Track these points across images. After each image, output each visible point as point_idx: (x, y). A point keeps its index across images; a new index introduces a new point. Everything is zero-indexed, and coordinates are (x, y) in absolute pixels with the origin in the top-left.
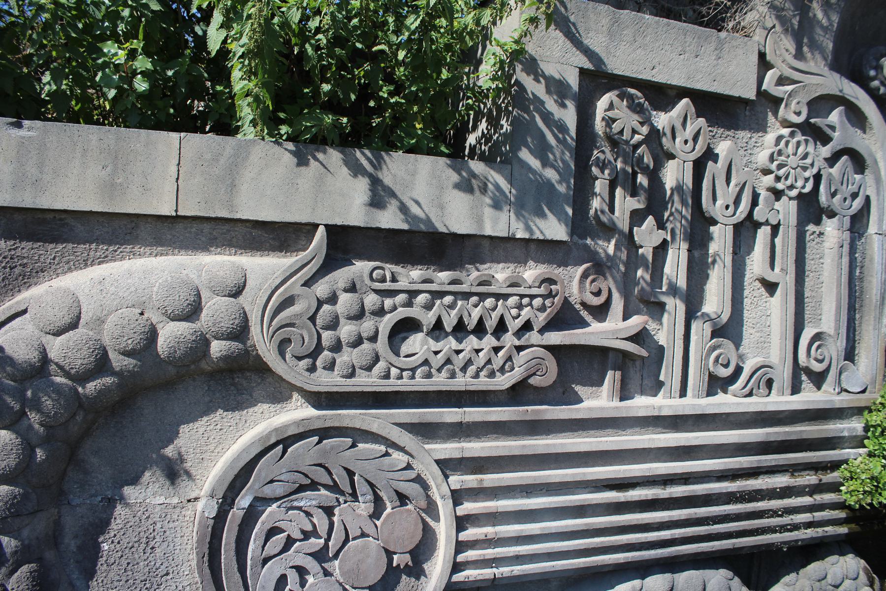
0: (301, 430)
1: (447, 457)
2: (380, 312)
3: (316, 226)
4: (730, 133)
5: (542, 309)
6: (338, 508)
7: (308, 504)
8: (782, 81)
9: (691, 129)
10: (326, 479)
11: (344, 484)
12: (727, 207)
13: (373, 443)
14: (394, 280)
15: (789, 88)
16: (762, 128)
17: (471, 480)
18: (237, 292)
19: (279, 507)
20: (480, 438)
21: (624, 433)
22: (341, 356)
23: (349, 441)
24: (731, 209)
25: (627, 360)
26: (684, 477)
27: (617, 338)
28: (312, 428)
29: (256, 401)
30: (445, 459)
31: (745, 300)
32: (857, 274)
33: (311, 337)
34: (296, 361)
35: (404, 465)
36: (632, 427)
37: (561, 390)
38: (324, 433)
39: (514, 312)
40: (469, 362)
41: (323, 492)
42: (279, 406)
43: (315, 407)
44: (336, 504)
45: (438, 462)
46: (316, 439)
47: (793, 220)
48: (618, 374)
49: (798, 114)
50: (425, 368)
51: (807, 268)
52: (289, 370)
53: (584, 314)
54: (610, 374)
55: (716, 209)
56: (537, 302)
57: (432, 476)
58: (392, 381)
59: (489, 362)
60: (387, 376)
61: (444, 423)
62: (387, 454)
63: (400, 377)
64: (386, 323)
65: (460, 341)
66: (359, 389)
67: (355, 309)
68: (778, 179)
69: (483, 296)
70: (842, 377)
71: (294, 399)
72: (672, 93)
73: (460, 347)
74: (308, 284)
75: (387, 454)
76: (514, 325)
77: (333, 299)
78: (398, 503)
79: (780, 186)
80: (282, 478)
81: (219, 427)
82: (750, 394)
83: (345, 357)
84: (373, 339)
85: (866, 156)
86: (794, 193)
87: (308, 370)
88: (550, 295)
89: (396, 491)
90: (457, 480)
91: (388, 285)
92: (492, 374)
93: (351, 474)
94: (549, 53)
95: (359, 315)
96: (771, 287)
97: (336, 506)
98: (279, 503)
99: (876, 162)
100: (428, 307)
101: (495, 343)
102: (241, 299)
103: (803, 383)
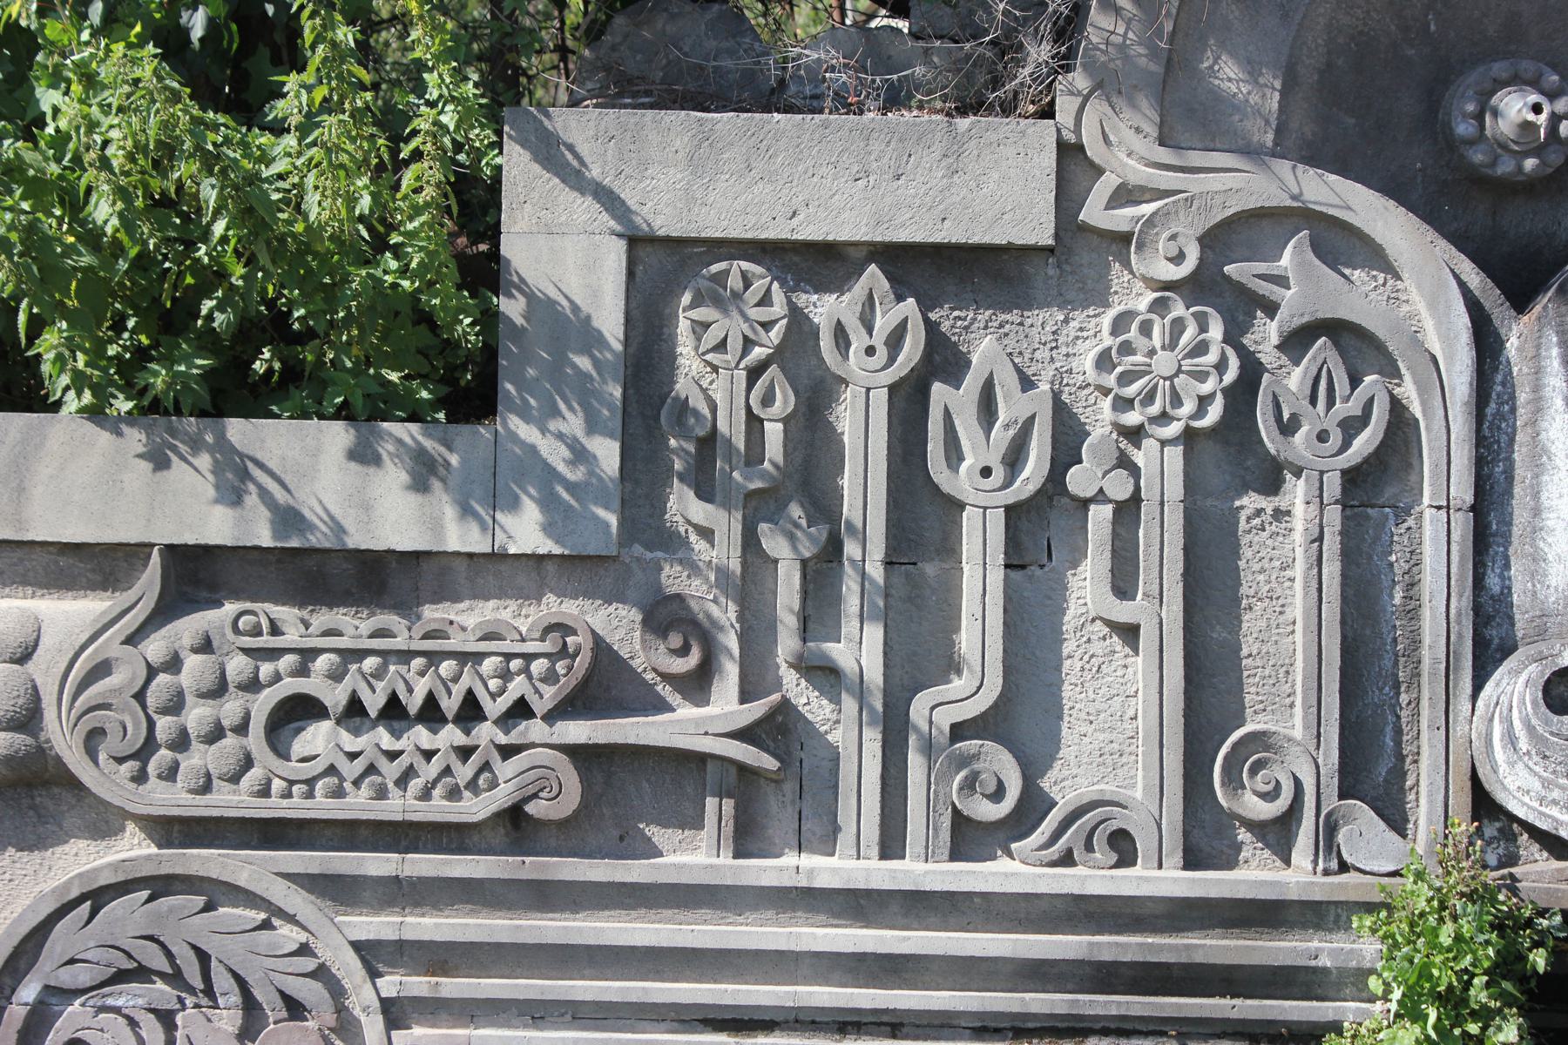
0: (121, 878)
1: (371, 937)
2: (253, 685)
3: (153, 545)
4: (1014, 316)
5: (550, 677)
6: (181, 1014)
7: (131, 1003)
8: (1125, 195)
9: (883, 323)
10: (161, 963)
11: (194, 978)
12: (986, 472)
13: (246, 907)
14: (275, 630)
15: (1147, 209)
16: (1101, 299)
17: (419, 985)
18: (24, 656)
19: (83, 1005)
20: (440, 910)
21: (740, 919)
22: (189, 758)
23: (200, 901)
24: (999, 474)
25: (762, 781)
26: (885, 1019)
27: (706, 733)
28: (138, 875)
29: (67, 834)
30: (368, 941)
31: (1067, 663)
32: (1397, 600)
33: (136, 725)
34: (113, 765)
35: (295, 947)
36: (755, 908)
37: (616, 833)
38: (162, 886)
39: (494, 684)
40: (409, 773)
41: (160, 985)
42: (104, 843)
43: (160, 847)
44: (178, 1006)
45: (357, 946)
46: (145, 894)
47: (1175, 488)
48: (728, 805)
49: (1178, 258)
50: (332, 781)
51: (1244, 590)
52: (102, 779)
53: (665, 690)
54: (711, 803)
55: (961, 482)
56: (538, 667)
57: (348, 967)
58: (274, 800)
59: (447, 771)
60: (265, 792)
61: (365, 877)
62: (266, 925)
63: (288, 795)
64: (263, 704)
65: (397, 735)
66: (215, 813)
67: (209, 681)
68: (1123, 404)
69: (433, 658)
70: (1341, 838)
71: (128, 834)
72: (854, 254)
73: (398, 746)
74: (132, 640)
75: (266, 925)
76: (494, 708)
77: (174, 664)
78: (284, 1014)
79: (1133, 418)
80: (88, 956)
81: (7, 876)
82: (1067, 860)
83: (196, 759)
84: (242, 728)
85: (1381, 333)
86: (1174, 429)
87: (134, 779)
88: (563, 652)
89: (282, 993)
90: (390, 985)
91: (266, 641)
92: (454, 794)
93: (203, 957)
94: (563, 219)
95: (219, 690)
96: (1129, 633)
97: (179, 1010)
98: (83, 998)
99: (1415, 341)
100: (336, 676)
101: (458, 738)
102: (30, 666)
103: (1245, 848)
